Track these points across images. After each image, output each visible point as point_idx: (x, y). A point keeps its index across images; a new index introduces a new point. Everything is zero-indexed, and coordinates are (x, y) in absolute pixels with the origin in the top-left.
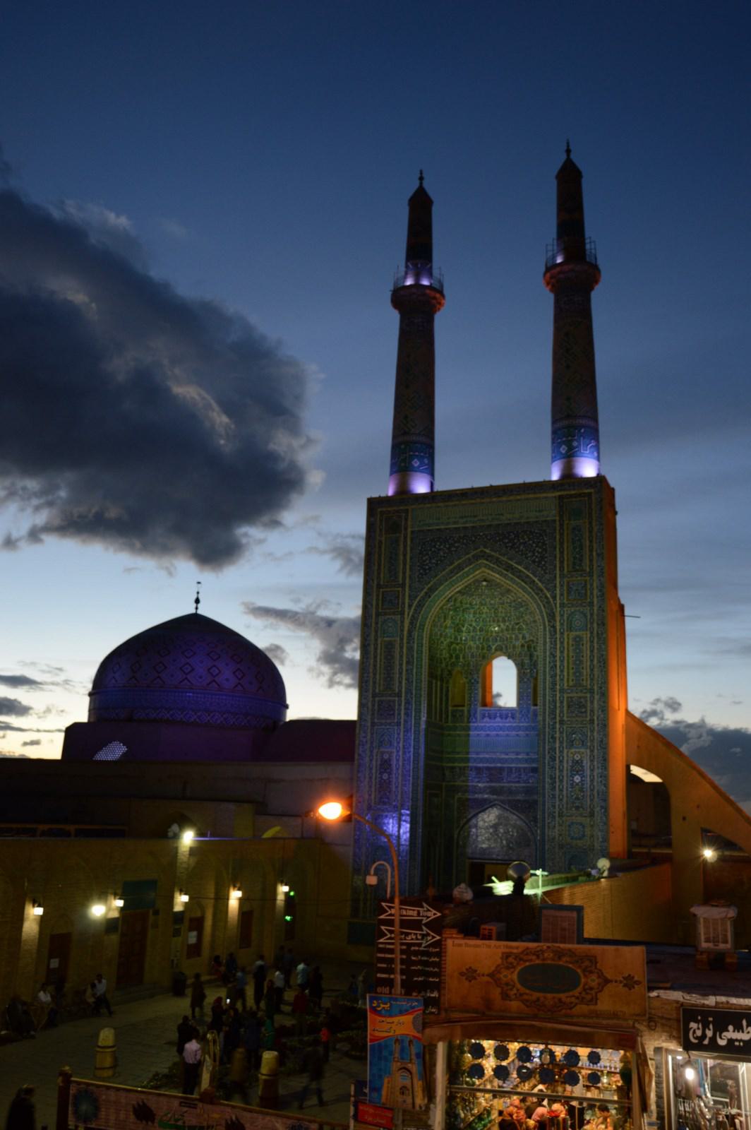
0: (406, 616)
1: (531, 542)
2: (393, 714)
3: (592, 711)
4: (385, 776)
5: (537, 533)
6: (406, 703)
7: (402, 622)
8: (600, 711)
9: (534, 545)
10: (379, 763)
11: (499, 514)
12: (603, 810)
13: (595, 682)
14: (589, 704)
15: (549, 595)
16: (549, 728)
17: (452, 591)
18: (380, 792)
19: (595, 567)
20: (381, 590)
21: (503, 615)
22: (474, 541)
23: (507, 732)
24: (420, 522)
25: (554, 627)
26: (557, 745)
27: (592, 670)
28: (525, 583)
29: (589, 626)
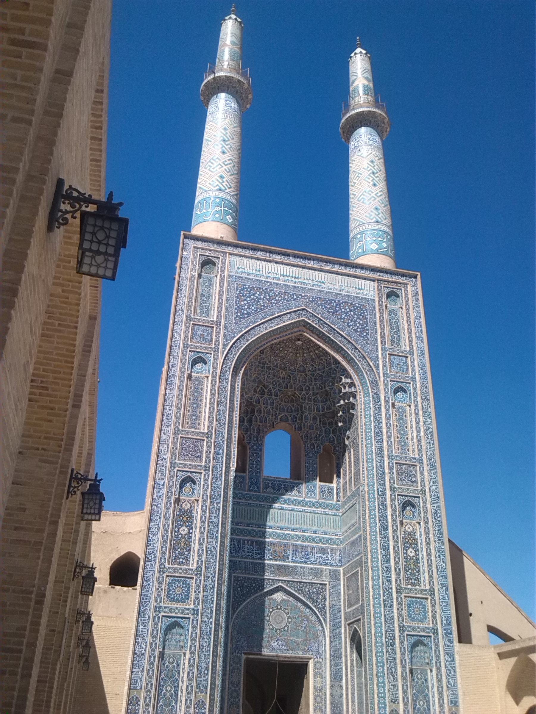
0: (220, 354)
1: (352, 313)
2: (201, 457)
3: (422, 481)
4: (184, 530)
5: (358, 307)
6: (215, 446)
7: (216, 359)
8: (432, 482)
9: (356, 316)
10: (177, 512)
11: (320, 282)
12: (444, 588)
13: (424, 453)
14: (419, 474)
15: (371, 364)
16: (378, 494)
17: (270, 342)
18: (174, 548)
19: (414, 348)
20: (191, 323)
21: (301, 384)
22: (295, 300)
23: (294, 507)
24: (238, 268)
25: (377, 394)
26: (389, 512)
27: (419, 441)
28: (347, 348)
29: (413, 399)
